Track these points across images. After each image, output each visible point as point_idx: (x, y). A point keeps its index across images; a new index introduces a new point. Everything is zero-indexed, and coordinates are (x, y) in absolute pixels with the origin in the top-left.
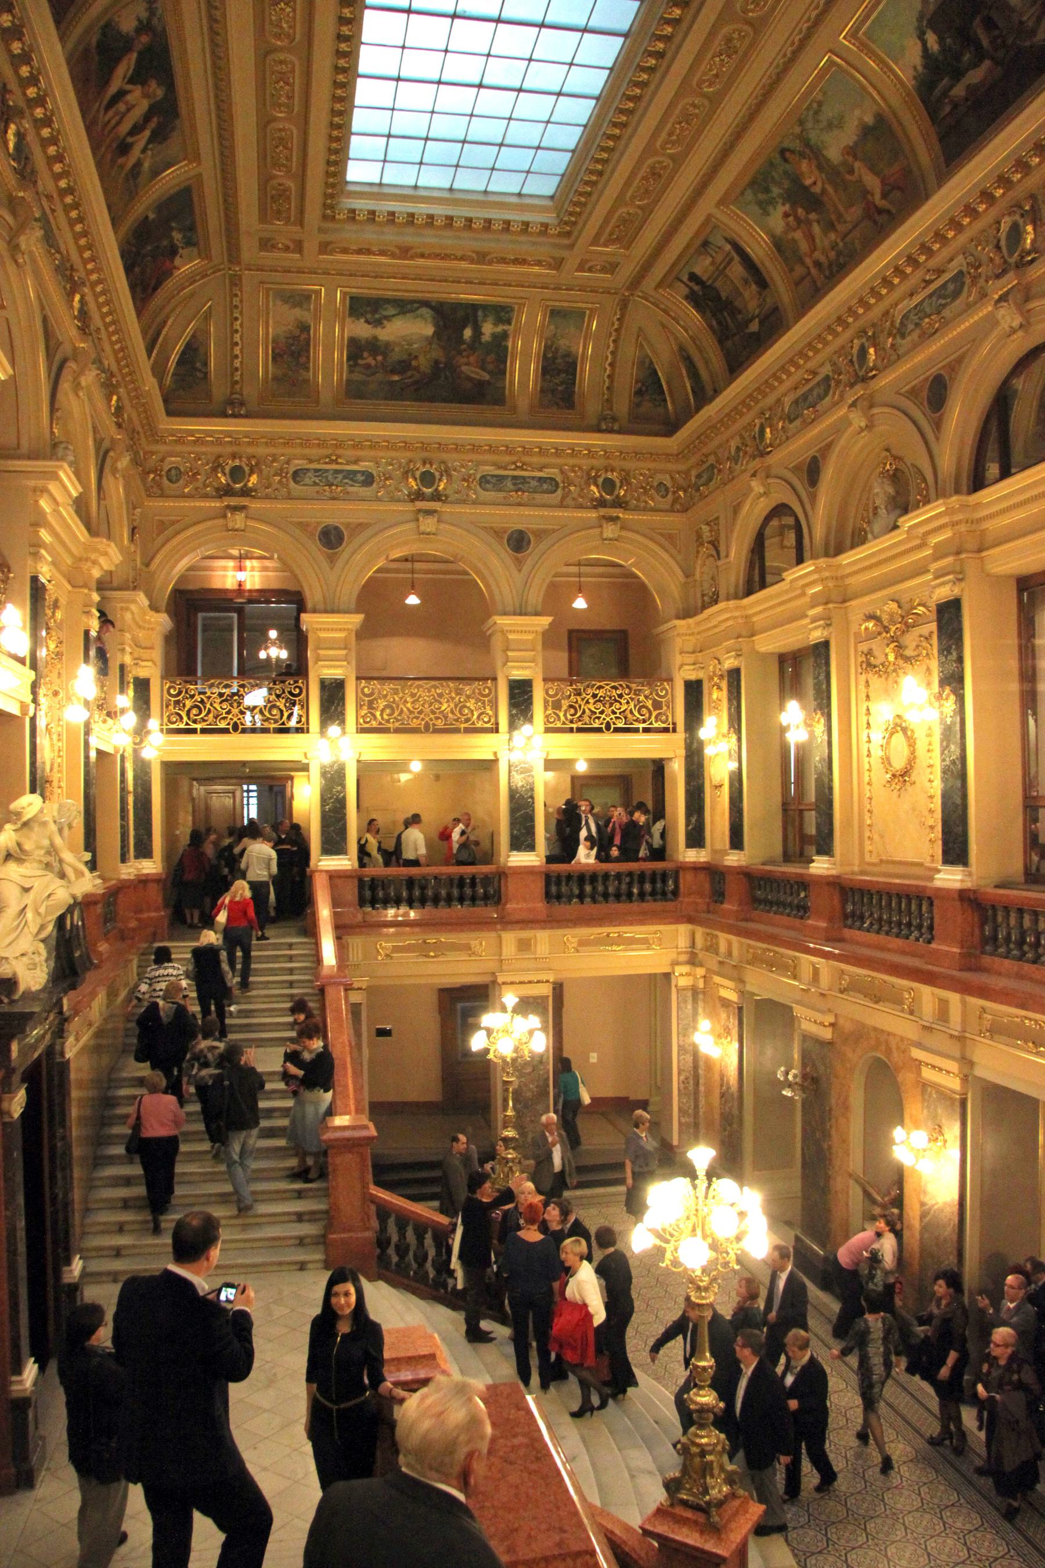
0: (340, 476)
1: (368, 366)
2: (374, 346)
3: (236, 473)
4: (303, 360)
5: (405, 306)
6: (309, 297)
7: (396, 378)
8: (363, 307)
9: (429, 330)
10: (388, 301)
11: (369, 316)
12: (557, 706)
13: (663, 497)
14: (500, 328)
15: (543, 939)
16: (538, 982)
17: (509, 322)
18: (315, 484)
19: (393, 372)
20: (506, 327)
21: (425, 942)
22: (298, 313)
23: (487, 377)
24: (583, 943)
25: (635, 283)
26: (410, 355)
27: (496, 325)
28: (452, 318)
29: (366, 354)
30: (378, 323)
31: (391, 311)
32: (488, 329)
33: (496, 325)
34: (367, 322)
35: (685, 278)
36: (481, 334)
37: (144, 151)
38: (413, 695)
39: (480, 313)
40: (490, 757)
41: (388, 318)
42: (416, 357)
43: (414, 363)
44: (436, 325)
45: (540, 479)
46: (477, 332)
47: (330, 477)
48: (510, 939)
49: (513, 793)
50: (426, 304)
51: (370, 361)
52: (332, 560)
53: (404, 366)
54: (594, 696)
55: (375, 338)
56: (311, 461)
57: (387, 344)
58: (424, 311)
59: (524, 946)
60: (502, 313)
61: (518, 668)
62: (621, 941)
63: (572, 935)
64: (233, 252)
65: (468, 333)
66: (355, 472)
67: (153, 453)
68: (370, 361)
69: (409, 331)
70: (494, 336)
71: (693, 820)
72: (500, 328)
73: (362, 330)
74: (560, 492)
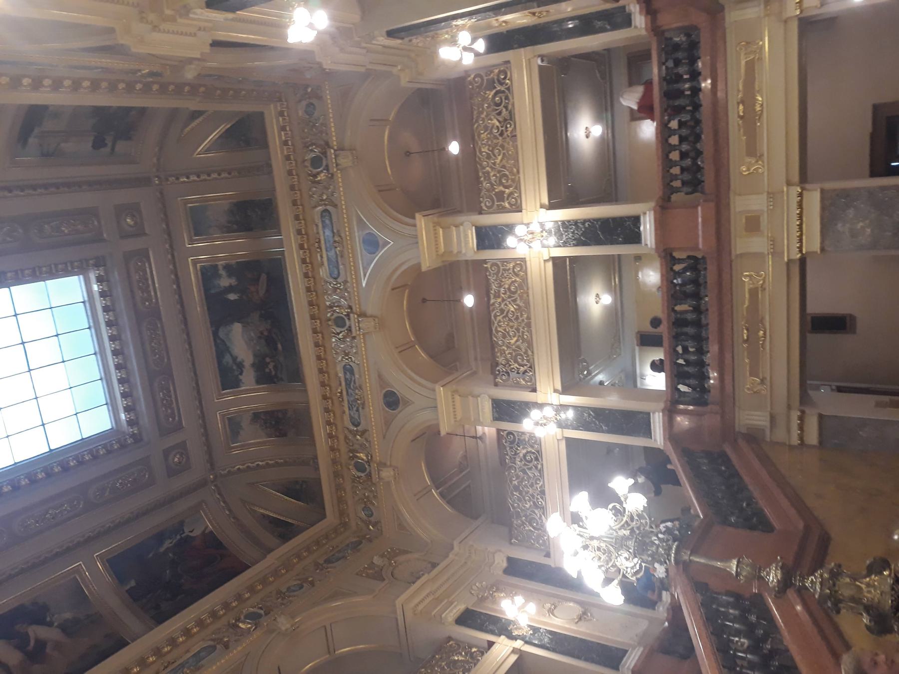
0: (350, 391)
1: (275, 367)
2: (259, 366)
3: (360, 467)
4: (280, 415)
5: (221, 348)
6: (229, 419)
7: (279, 346)
8: (229, 378)
9: (237, 327)
10: (220, 363)
11: (236, 373)
12: (500, 196)
13: (314, 108)
14: (222, 272)
15: (744, 204)
16: (800, 205)
17: (215, 267)
18: (357, 410)
19: (276, 349)
20: (220, 268)
21: (746, 341)
22: (245, 423)
23: (264, 277)
24: (752, 150)
25: (142, 181)
26: (260, 338)
27: (220, 276)
28: (221, 312)
29: (267, 370)
30: (240, 366)
31: (228, 359)
32: (225, 282)
33: (220, 276)
34: (241, 374)
35: (108, 150)
36: (231, 286)
37: (50, 625)
38: (504, 337)
39: (213, 291)
40: (550, 265)
41: (234, 359)
42: (262, 333)
43: (266, 333)
44: (232, 322)
45: (324, 227)
46: (230, 289)
47: (352, 399)
48: (744, 244)
49: (579, 243)
50: (215, 334)
51: (271, 366)
52: (407, 403)
53: (270, 341)
54: (489, 157)
55: (253, 365)
56: (344, 412)
57: (255, 356)
58: (221, 334)
59: (753, 224)
60: (208, 274)
61: (467, 243)
62: (748, 100)
63: (741, 167)
64: (203, 484)
65: (232, 297)
66: (346, 379)
67: (357, 524)
68: (271, 366)
69: (241, 342)
70: (230, 276)
71: (599, 24)
72: (222, 272)
73: (248, 377)
74: (329, 208)
